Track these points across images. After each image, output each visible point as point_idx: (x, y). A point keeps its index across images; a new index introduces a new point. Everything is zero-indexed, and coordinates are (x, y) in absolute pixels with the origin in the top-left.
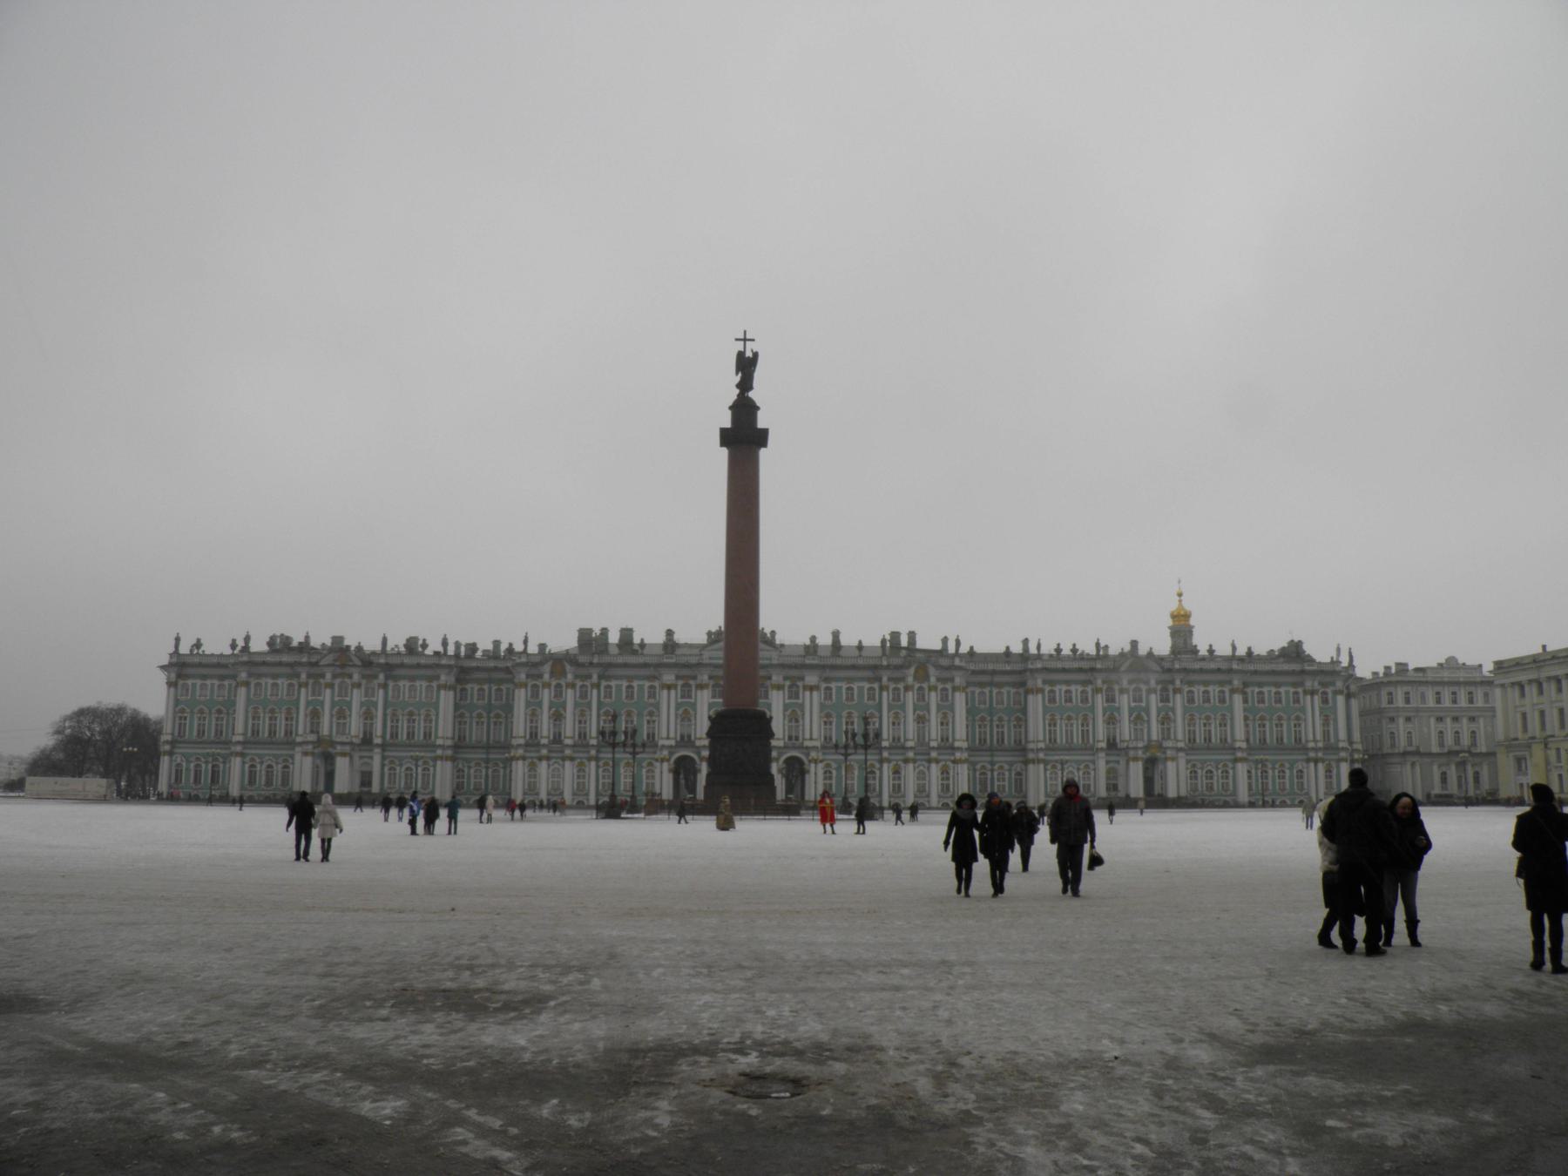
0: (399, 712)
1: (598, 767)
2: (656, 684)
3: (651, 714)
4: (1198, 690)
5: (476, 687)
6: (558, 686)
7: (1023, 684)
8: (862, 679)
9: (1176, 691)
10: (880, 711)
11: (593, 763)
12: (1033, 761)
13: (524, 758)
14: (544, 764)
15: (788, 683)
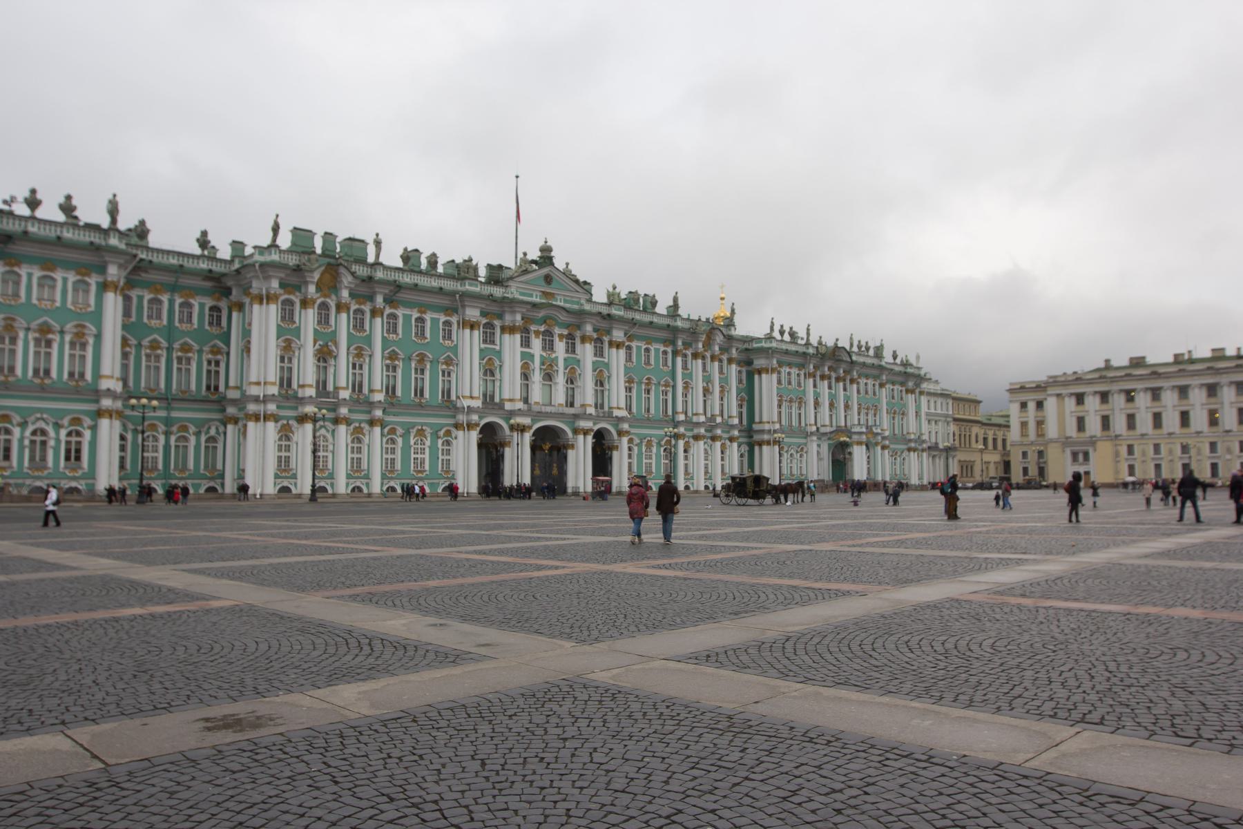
0: (21, 323)
1: (382, 435)
2: (454, 319)
3: (449, 362)
4: (863, 381)
5: (148, 296)
6: (324, 306)
7: (749, 363)
8: (657, 340)
9: (852, 381)
10: (674, 379)
11: (377, 430)
12: (768, 443)
13: (276, 418)
14: (309, 427)
15: (595, 336)
